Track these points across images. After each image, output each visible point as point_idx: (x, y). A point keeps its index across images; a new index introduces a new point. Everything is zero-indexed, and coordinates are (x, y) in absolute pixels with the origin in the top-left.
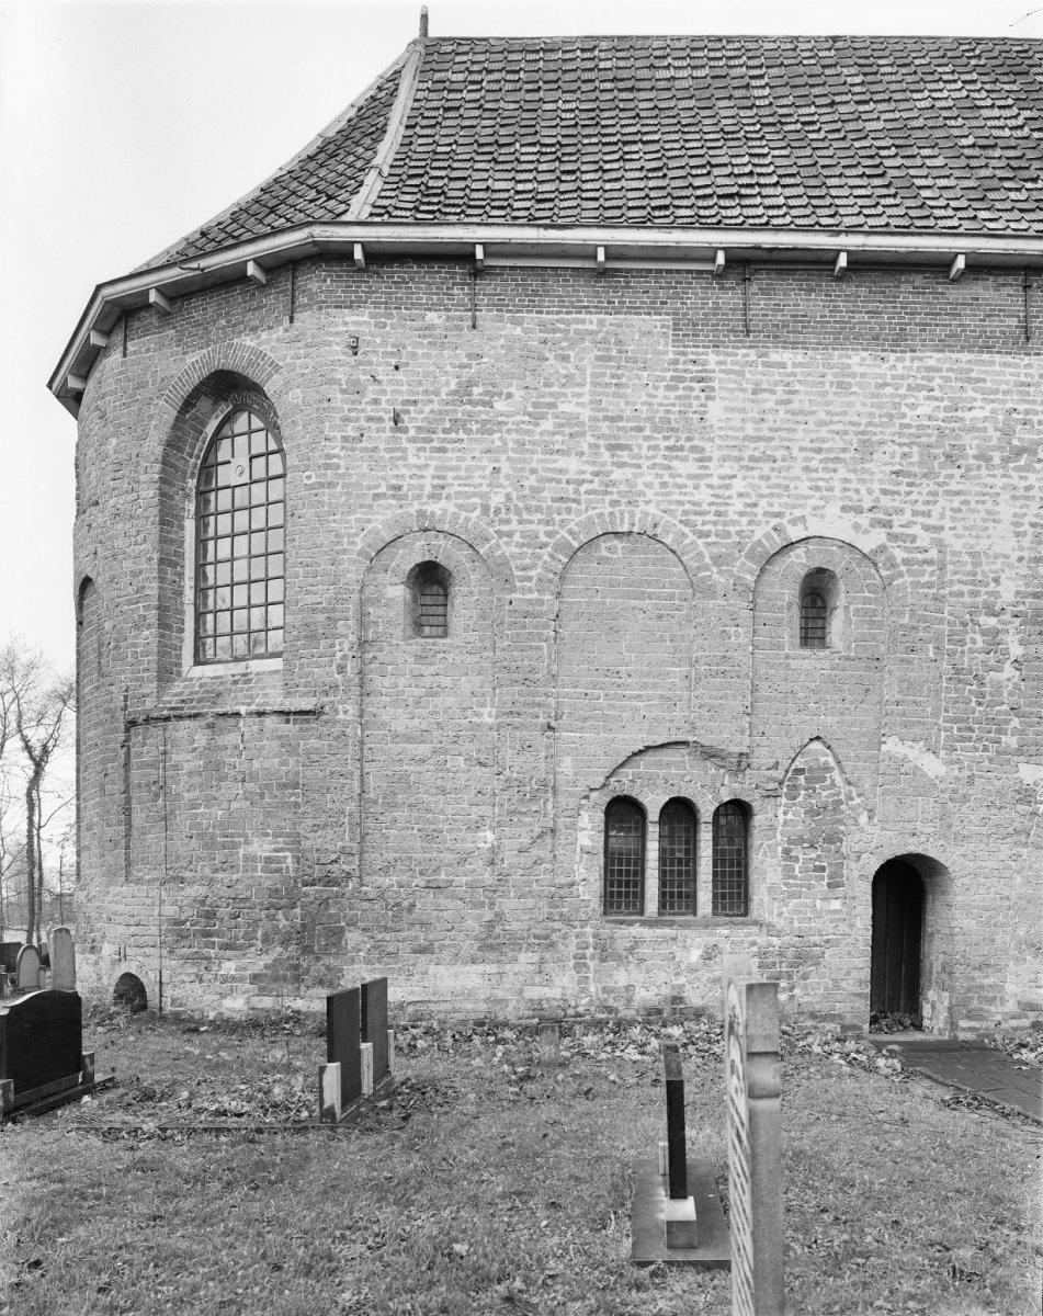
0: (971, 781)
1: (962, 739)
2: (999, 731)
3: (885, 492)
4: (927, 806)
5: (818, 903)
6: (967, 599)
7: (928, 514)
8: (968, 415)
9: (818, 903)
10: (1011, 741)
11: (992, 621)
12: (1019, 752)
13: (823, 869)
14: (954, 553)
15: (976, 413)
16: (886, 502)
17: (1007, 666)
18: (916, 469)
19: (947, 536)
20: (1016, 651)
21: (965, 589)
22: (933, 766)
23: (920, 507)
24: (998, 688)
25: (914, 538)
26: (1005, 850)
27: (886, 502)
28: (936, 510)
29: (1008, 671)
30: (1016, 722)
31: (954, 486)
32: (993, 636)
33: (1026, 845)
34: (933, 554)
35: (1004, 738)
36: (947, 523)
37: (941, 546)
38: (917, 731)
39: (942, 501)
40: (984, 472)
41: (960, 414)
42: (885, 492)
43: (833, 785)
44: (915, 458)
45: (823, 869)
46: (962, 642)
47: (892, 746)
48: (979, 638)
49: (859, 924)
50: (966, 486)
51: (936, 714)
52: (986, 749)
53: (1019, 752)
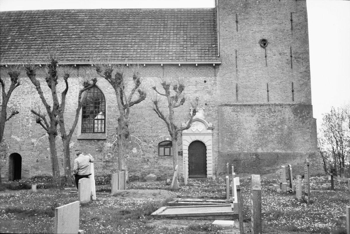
0: (24, 142)
1: (23, 135)
2: (29, 134)
3: (13, 98)
4: (18, 145)
5: (2, 161)
6: (24, 114)
7: (19, 102)
8: (26, 87)
9: (2, 161)
10: (30, 135)
11: (27, 118)
12: (32, 137)
13: (3, 155)
14: (23, 107)
15: (27, 86)
16: (13, 100)
17: (30, 124)
18: (18, 95)
19: (21, 105)
20: (31, 122)
21: (24, 113)
22: (18, 139)
23: (18, 100)
24: (28, 127)
25: (16, 105)
26: (30, 152)
27: (13, 100)
28: (20, 101)
29: (30, 125)
30: (31, 132)
31: (23, 97)
32: (27, 120)
33: (33, 151)
34: (19, 107)
35: (29, 135)
36: (22, 103)
37: (21, 106)
38: (16, 134)
39: (21, 100)
40: (28, 95)
41: (25, 87)
42: (13, 98)
43: (5, 142)
44: (18, 93)
45: (3, 155)
46: (23, 121)
47: (12, 136)
48: (26, 120)
49: (7, 164)
50: (26, 97)
51: (19, 132)
52: (26, 137)
53: (32, 137)
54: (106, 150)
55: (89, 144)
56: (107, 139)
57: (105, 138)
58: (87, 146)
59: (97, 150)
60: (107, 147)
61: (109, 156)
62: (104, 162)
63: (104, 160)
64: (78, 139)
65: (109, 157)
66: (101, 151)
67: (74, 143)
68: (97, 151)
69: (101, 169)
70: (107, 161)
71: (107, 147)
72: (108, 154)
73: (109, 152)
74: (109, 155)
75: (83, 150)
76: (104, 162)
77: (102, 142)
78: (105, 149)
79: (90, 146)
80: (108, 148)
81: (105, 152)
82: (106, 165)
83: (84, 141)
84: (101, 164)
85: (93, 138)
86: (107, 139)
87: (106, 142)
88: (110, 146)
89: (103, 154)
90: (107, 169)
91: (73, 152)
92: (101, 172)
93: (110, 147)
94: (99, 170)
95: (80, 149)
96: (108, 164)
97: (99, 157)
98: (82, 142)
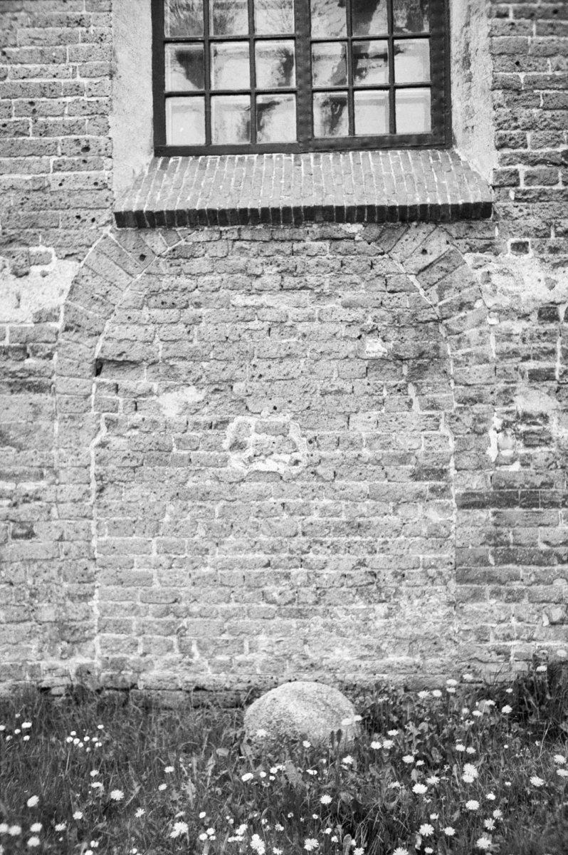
54: (492, 348)
55: (270, 277)
56: (499, 206)
57: (475, 195)
58: (239, 299)
59: (374, 347)
60: (504, 313)
61: (529, 430)
62: (470, 502)
63: (477, 483)
64: (122, 219)
65: (528, 439)
66: (422, 365)
67: (70, 269)
68: (377, 364)
69: (439, 596)
70: (504, 497)
71: (504, 313)
72: (520, 405)
73: (535, 376)
74: (525, 417)
75: (194, 357)
76: (470, 502)
77: (438, 243)
78: (481, 338)
79: (282, 304)
80: (518, 327)
81: (477, 373)
82: (494, 539)
83: (202, 235)
84: (437, 536)
85: (313, 200)
86: (506, 203)
87: (489, 247)
88: (545, 295)
89: (448, 396)
90: (514, 597)
91: (60, 384)
92: (430, 627)
93: (548, 313)
94: (409, 609)
95: (159, 350)
96: (525, 534)
97: (405, 441)
98: (176, 256)
